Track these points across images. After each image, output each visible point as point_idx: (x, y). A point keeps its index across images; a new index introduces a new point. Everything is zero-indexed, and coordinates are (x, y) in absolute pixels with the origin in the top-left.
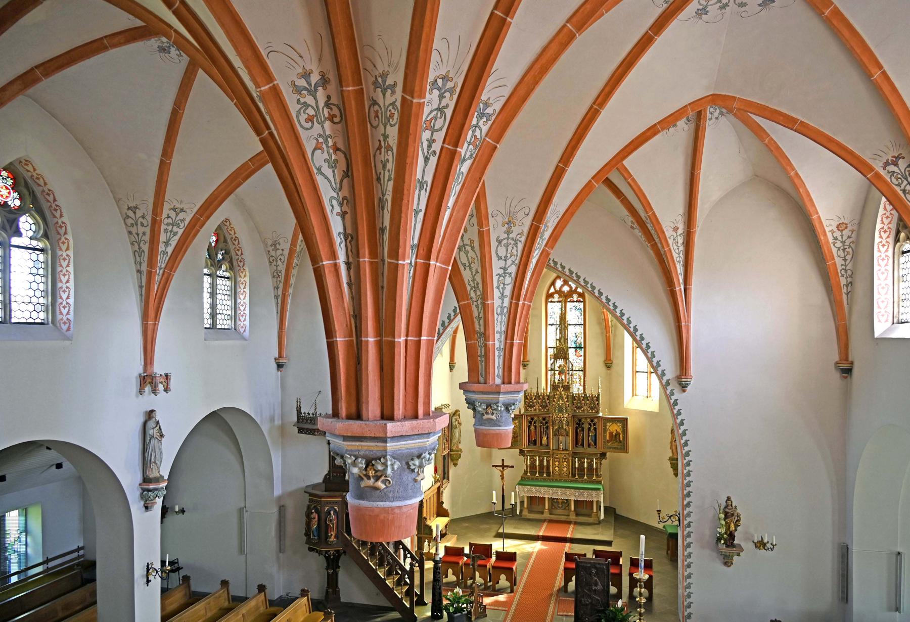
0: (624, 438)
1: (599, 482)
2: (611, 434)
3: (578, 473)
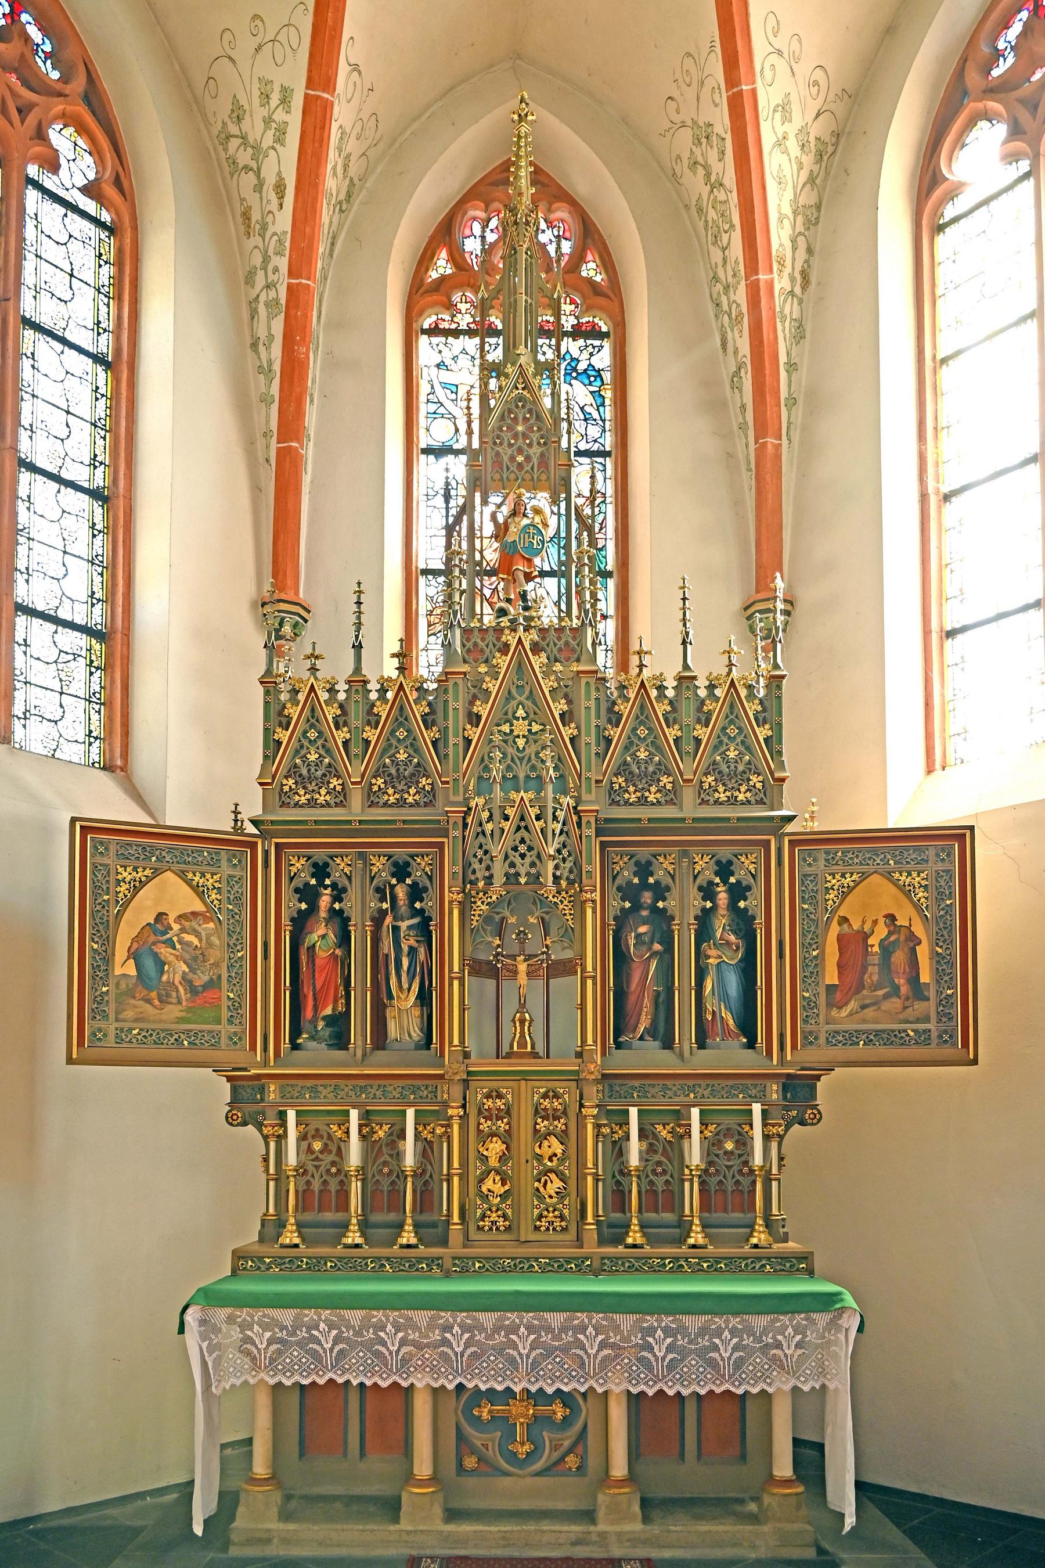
1: (802, 1264)
3: (639, 1215)
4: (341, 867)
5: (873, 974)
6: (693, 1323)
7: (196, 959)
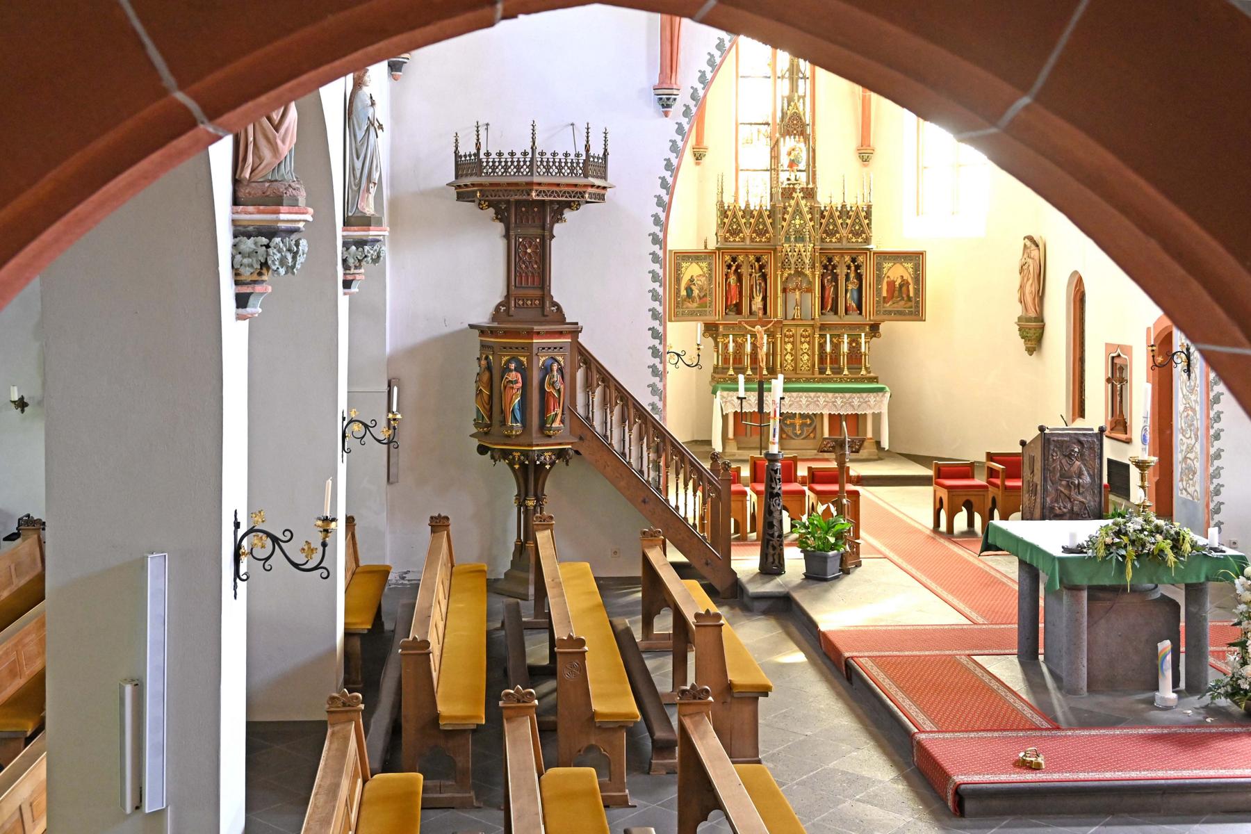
0: (917, 291)
2: (891, 284)
3: (827, 363)
4: (741, 258)
5: (896, 293)
6: (847, 395)
7: (701, 289)
